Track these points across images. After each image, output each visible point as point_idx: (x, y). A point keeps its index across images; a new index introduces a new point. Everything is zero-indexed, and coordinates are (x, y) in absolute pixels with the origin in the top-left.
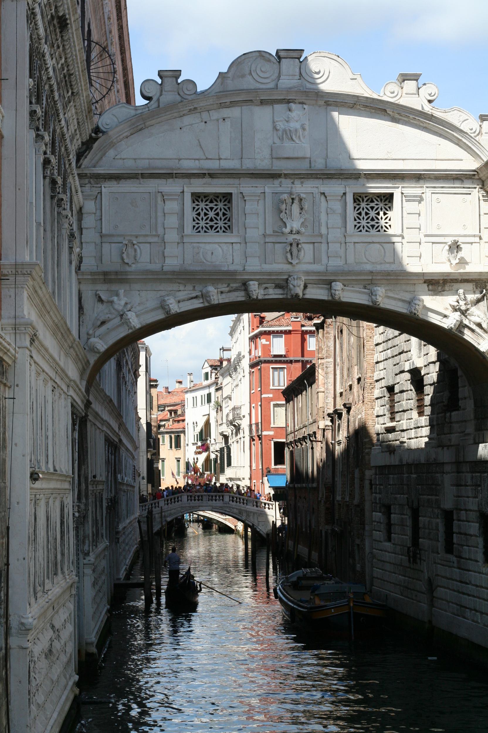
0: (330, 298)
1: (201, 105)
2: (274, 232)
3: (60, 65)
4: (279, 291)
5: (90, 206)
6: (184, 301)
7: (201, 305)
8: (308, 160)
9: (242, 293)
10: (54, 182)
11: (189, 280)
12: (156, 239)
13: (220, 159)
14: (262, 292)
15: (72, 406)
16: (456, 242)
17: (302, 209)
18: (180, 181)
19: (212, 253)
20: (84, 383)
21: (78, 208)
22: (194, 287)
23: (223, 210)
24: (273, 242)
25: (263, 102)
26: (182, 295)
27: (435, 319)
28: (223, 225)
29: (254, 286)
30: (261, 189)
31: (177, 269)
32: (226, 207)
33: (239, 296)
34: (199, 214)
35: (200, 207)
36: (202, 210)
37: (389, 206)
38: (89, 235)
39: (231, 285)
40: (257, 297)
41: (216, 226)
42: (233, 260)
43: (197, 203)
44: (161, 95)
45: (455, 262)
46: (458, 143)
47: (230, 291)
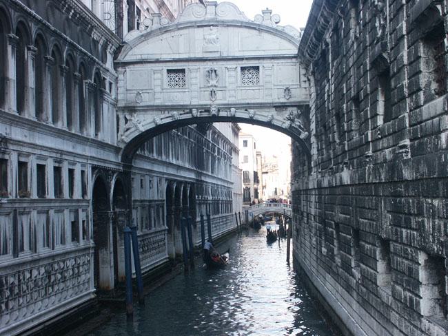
3: (71, 14)
5: (121, 77)
10: (61, 67)
11: (165, 110)
12: (150, 91)
15: (94, 168)
16: (287, 88)
17: (216, 75)
18: (161, 64)
20: (120, 157)
21: (114, 78)
25: (199, 27)
26: (162, 116)
27: (279, 124)
29: (194, 111)
31: (160, 104)
33: (189, 116)
38: (120, 90)
45: (287, 98)
46: (290, 41)
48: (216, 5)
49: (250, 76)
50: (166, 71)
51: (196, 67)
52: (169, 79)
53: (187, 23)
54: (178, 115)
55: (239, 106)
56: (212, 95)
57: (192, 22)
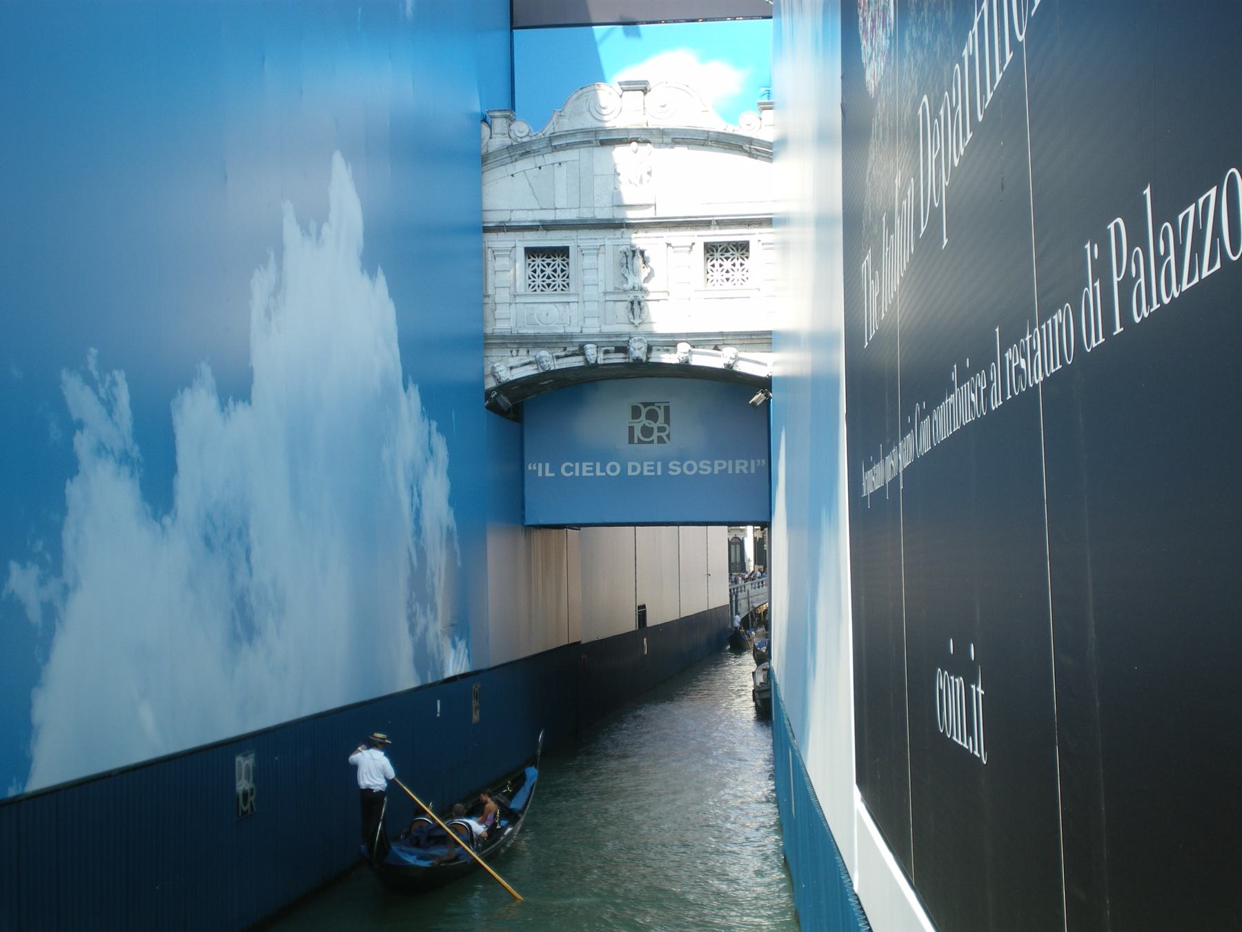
0: (677, 362)
1: (534, 148)
2: (615, 288)
4: (622, 355)
6: (516, 367)
7: (535, 372)
8: (654, 207)
9: (581, 358)
13: (556, 209)
14: (601, 356)
18: (512, 235)
19: (547, 314)
22: (528, 352)
23: (561, 266)
24: (614, 301)
25: (603, 143)
26: (514, 361)
28: (561, 283)
29: (591, 350)
30: (600, 241)
32: (564, 263)
33: (576, 362)
34: (535, 271)
35: (536, 263)
36: (538, 266)
37: (746, 255)
39: (568, 349)
40: (596, 361)
41: (553, 283)
42: (570, 321)
43: (533, 258)
44: (491, 138)
47: (566, 356)
48: (645, 91)
49: (727, 264)
50: (523, 249)
51: (598, 243)
52: (530, 272)
53: (574, 133)
54: (551, 361)
55: (699, 340)
56: (632, 310)
57: (585, 132)
